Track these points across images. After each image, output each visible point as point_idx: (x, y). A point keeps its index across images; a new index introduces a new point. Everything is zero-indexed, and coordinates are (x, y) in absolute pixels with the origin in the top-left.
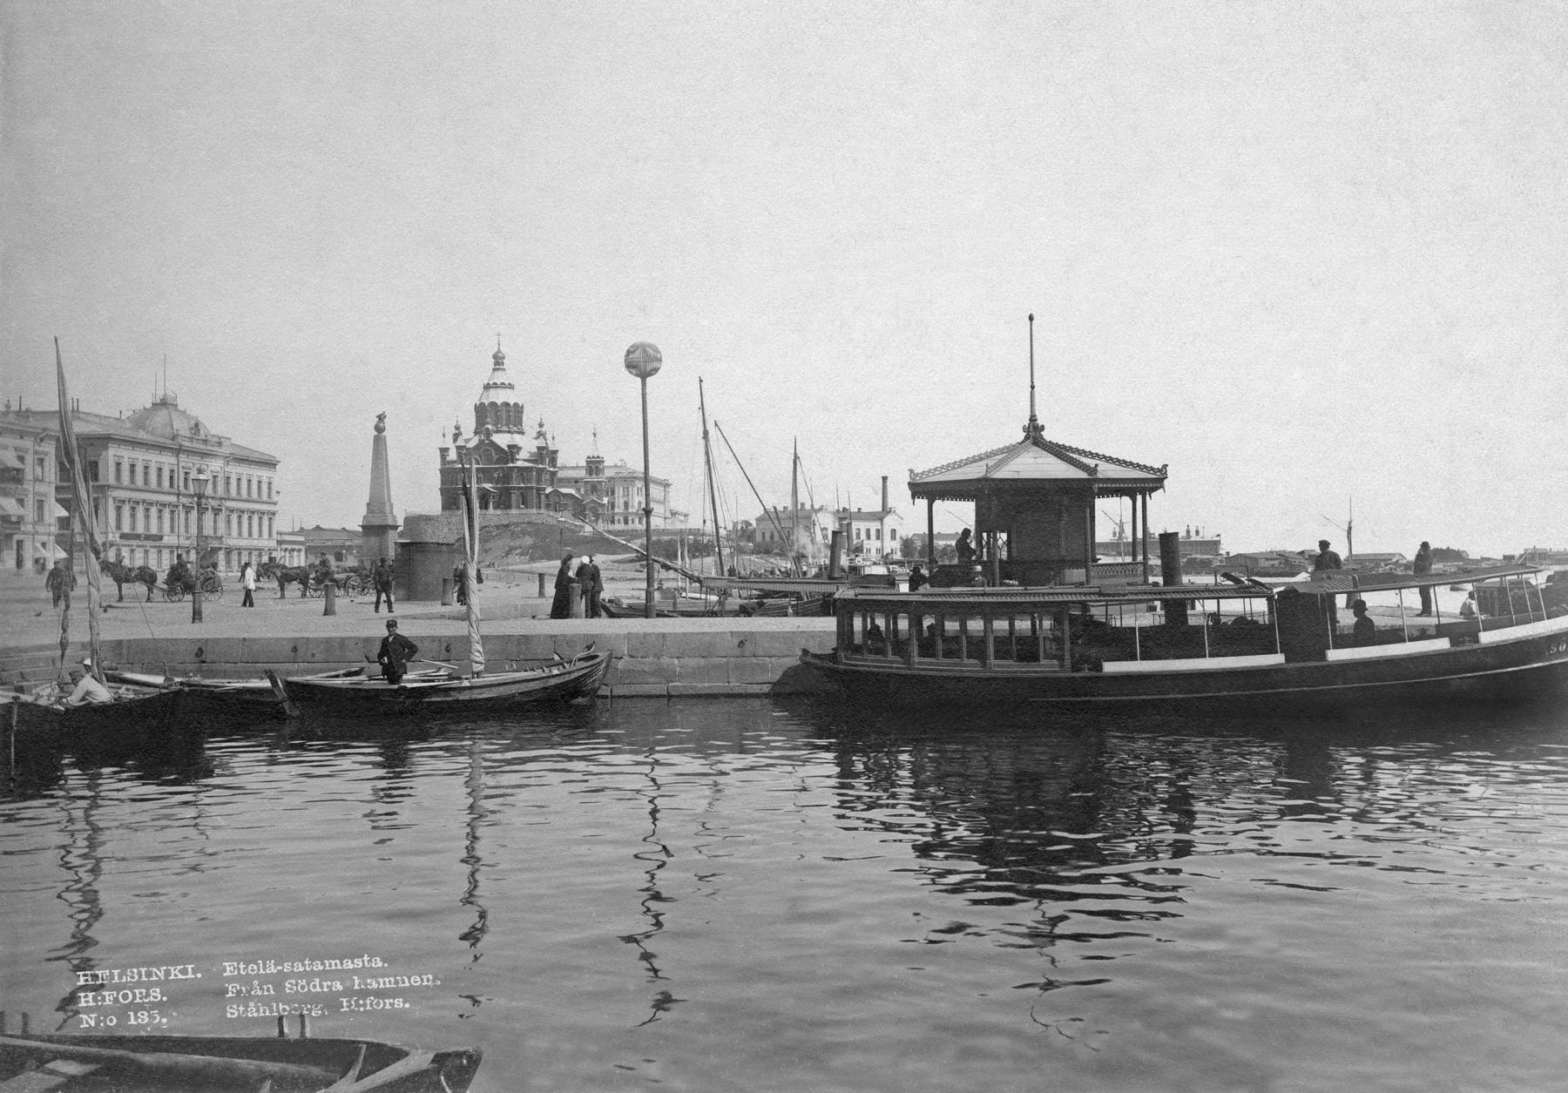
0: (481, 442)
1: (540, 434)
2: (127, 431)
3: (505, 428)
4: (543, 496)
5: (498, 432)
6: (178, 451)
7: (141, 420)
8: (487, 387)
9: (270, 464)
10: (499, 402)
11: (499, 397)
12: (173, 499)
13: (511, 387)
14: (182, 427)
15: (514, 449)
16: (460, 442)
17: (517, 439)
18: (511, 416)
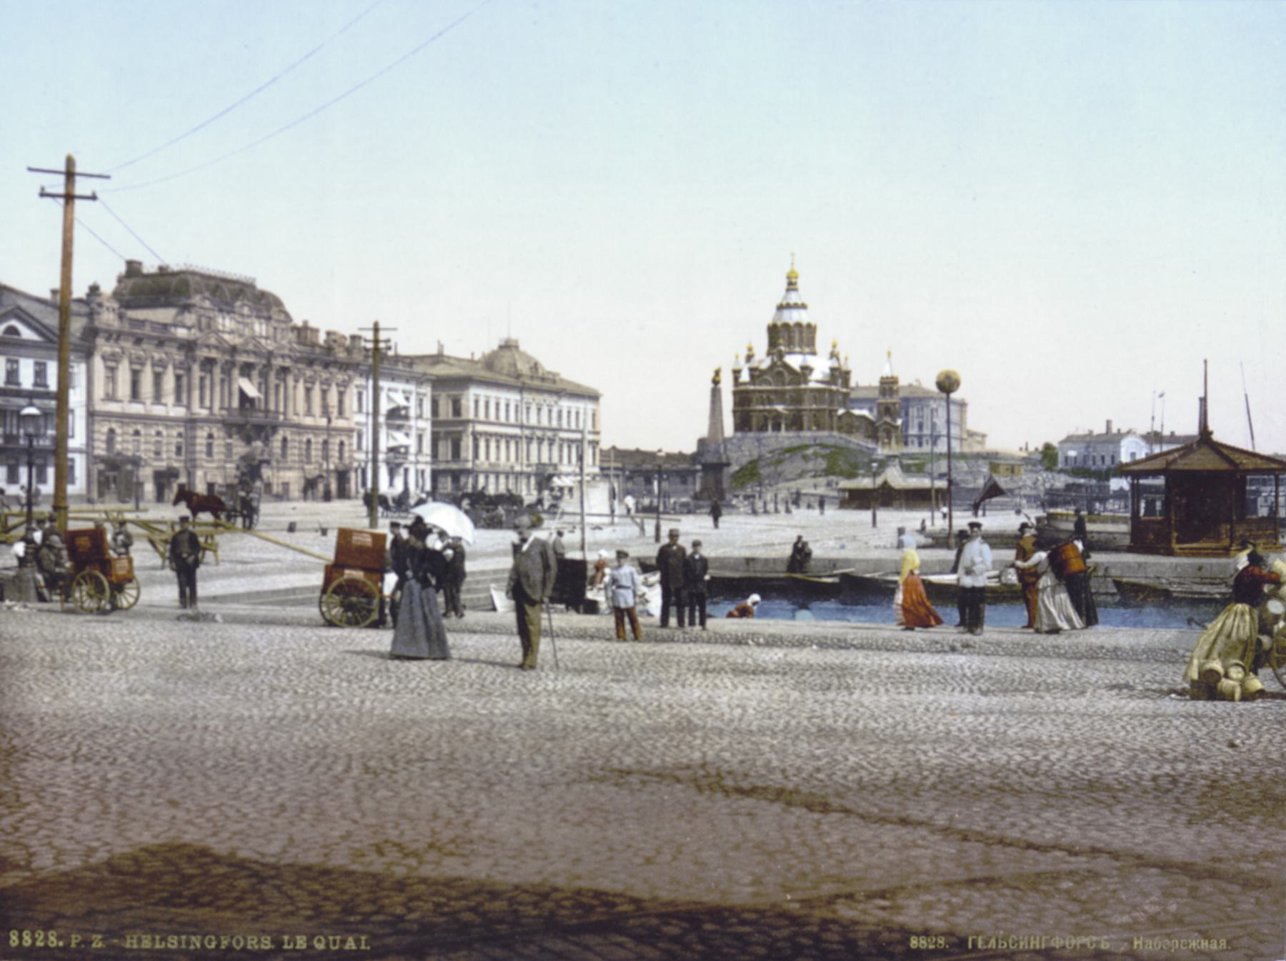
0: (773, 365)
1: (833, 355)
2: (483, 373)
3: (797, 349)
4: (835, 419)
5: (790, 353)
6: (522, 389)
7: (490, 362)
8: (781, 308)
9: (594, 397)
10: (791, 323)
11: (793, 317)
12: (517, 431)
13: (803, 306)
14: (523, 368)
15: (807, 370)
16: (754, 364)
17: (811, 361)
18: (803, 336)
